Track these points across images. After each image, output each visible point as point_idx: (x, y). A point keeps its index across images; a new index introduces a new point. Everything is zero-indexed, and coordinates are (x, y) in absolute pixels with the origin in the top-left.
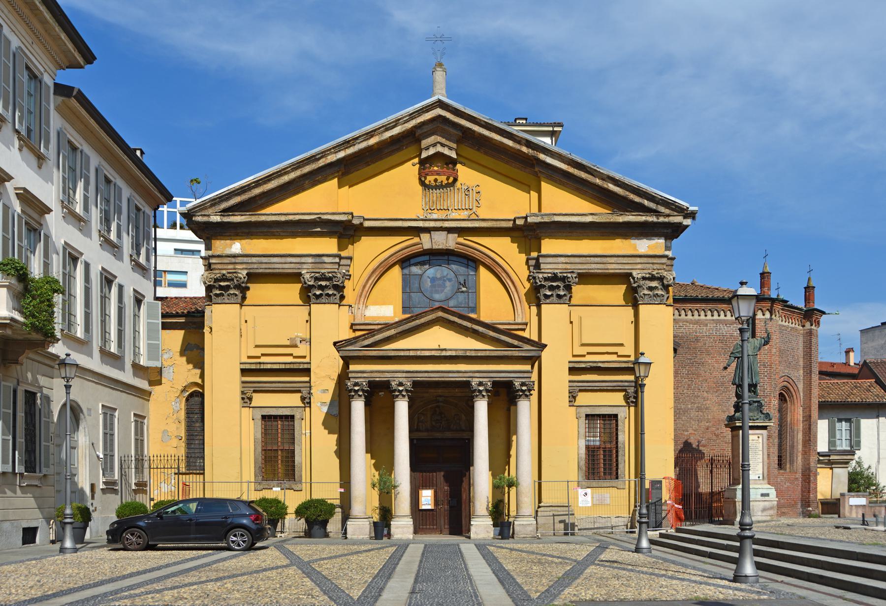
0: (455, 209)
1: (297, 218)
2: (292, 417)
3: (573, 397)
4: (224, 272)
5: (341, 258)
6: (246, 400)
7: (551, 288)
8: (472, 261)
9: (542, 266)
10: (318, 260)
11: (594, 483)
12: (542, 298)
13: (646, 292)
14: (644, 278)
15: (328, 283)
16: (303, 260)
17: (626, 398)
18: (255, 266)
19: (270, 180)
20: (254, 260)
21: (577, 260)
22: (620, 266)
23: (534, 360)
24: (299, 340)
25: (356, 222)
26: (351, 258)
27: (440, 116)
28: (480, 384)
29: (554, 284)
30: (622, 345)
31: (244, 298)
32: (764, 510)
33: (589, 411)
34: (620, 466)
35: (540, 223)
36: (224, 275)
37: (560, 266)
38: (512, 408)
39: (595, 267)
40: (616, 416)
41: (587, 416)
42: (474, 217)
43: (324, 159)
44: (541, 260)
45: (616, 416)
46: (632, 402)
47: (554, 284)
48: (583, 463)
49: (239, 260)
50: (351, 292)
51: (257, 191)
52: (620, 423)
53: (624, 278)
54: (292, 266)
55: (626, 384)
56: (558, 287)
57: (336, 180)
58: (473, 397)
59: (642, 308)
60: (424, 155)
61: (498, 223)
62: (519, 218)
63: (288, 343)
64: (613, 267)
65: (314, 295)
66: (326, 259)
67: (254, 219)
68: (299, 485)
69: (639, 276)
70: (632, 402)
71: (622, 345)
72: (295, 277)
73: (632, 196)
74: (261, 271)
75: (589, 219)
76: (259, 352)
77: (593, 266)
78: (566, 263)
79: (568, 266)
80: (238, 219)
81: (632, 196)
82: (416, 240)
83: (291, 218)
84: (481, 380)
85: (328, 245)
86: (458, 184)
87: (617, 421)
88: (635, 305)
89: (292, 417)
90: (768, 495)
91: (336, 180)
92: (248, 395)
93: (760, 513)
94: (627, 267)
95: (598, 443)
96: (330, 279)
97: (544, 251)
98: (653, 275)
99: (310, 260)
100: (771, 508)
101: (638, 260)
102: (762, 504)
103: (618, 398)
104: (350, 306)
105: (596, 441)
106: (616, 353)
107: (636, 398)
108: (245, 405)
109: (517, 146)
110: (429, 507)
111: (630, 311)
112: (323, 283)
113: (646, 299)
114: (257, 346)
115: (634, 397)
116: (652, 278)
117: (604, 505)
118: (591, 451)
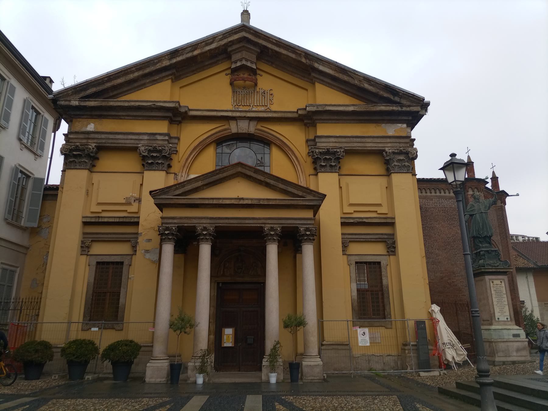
0: (255, 106)
1: (137, 104)
2: (122, 263)
3: (345, 246)
4: (78, 144)
5: (171, 138)
8: (266, 142)
9: (318, 144)
10: (152, 138)
13: (396, 164)
14: (394, 153)
15: (158, 155)
16: (141, 137)
18: (104, 141)
19: (119, 77)
20: (103, 136)
21: (344, 140)
22: (375, 145)
23: (316, 208)
24: (133, 199)
25: (183, 110)
28: (272, 229)
29: (327, 157)
31: (94, 166)
32: (518, 350)
33: (358, 259)
36: (77, 146)
37: (331, 145)
38: (298, 255)
39: (356, 145)
40: (379, 263)
41: (356, 263)
42: (268, 110)
43: (160, 64)
44: (317, 140)
45: (379, 263)
47: (327, 157)
48: (356, 304)
49: (92, 136)
50: (177, 164)
51: (109, 85)
52: (383, 270)
53: (379, 153)
54: (132, 141)
55: (386, 237)
56: (330, 159)
57: (170, 81)
58: (265, 242)
60: (233, 66)
61: (286, 114)
62: (300, 109)
63: (124, 201)
64: (370, 145)
65: (147, 163)
66: (159, 137)
69: (390, 151)
71: (380, 205)
72: (135, 149)
74: (108, 145)
75: (351, 109)
76: (99, 209)
77: (356, 145)
78: (336, 142)
83: (133, 104)
84: (272, 226)
85: (161, 127)
87: (380, 268)
89: (122, 263)
90: (517, 336)
92: (87, 244)
93: (515, 354)
94: (380, 145)
95: (367, 287)
96: (160, 151)
98: (401, 150)
99: (146, 137)
100: (524, 349)
101: (388, 140)
102: (516, 344)
104: (175, 174)
105: (365, 285)
106: (377, 211)
110: (230, 345)
112: (155, 155)
113: (396, 169)
114: (99, 204)
115: (392, 248)
116: (401, 153)
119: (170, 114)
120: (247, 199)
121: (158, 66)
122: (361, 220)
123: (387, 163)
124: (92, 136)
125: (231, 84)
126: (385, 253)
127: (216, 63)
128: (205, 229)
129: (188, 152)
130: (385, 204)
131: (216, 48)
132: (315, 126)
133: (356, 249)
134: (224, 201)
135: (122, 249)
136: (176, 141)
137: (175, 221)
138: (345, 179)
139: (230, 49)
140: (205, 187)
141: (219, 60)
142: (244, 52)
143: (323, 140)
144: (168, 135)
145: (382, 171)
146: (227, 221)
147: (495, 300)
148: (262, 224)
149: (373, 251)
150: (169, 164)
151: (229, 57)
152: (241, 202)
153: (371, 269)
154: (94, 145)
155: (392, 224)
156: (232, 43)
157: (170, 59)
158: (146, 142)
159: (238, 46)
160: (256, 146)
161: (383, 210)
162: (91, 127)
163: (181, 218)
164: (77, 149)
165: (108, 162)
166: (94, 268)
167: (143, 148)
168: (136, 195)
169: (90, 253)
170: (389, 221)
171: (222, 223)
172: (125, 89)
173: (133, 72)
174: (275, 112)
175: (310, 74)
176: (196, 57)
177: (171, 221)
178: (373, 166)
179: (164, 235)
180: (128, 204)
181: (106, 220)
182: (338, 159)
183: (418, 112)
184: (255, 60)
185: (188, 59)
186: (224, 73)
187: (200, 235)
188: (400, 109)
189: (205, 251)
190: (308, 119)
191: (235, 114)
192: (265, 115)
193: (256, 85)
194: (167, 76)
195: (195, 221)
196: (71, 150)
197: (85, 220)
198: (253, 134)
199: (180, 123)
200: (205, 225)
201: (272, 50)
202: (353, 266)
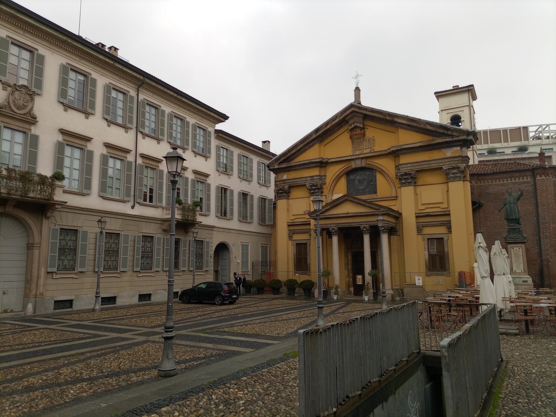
1: (303, 162)
5: (322, 176)
13: (451, 176)
14: (449, 169)
16: (307, 179)
20: (291, 181)
21: (416, 164)
25: (325, 161)
33: (429, 237)
37: (409, 168)
39: (425, 167)
41: (428, 239)
48: (427, 263)
49: (286, 181)
50: (326, 191)
51: (289, 154)
52: (445, 242)
64: (434, 166)
66: (315, 178)
71: (442, 203)
75: (418, 145)
79: (412, 168)
80: (283, 166)
85: (315, 172)
95: (435, 253)
96: (316, 186)
99: (309, 179)
101: (446, 160)
105: (434, 251)
113: (452, 179)
116: (454, 168)
118: (432, 257)
119: (319, 164)
121: (310, 139)
123: (447, 174)
124: (286, 181)
127: (341, 127)
128: (333, 229)
130: (446, 202)
133: (428, 231)
136: (324, 177)
138: (419, 189)
142: (356, 119)
143: (404, 166)
145: (445, 181)
154: (287, 186)
155: (449, 215)
157: (316, 134)
160: (367, 173)
162: (285, 177)
164: (280, 190)
165: (295, 193)
171: (341, 226)
173: (299, 145)
174: (375, 152)
176: (329, 128)
182: (414, 178)
185: (324, 132)
188: (451, 139)
189: (335, 239)
190: (395, 154)
192: (369, 155)
196: (278, 191)
199: (325, 166)
202: (426, 241)
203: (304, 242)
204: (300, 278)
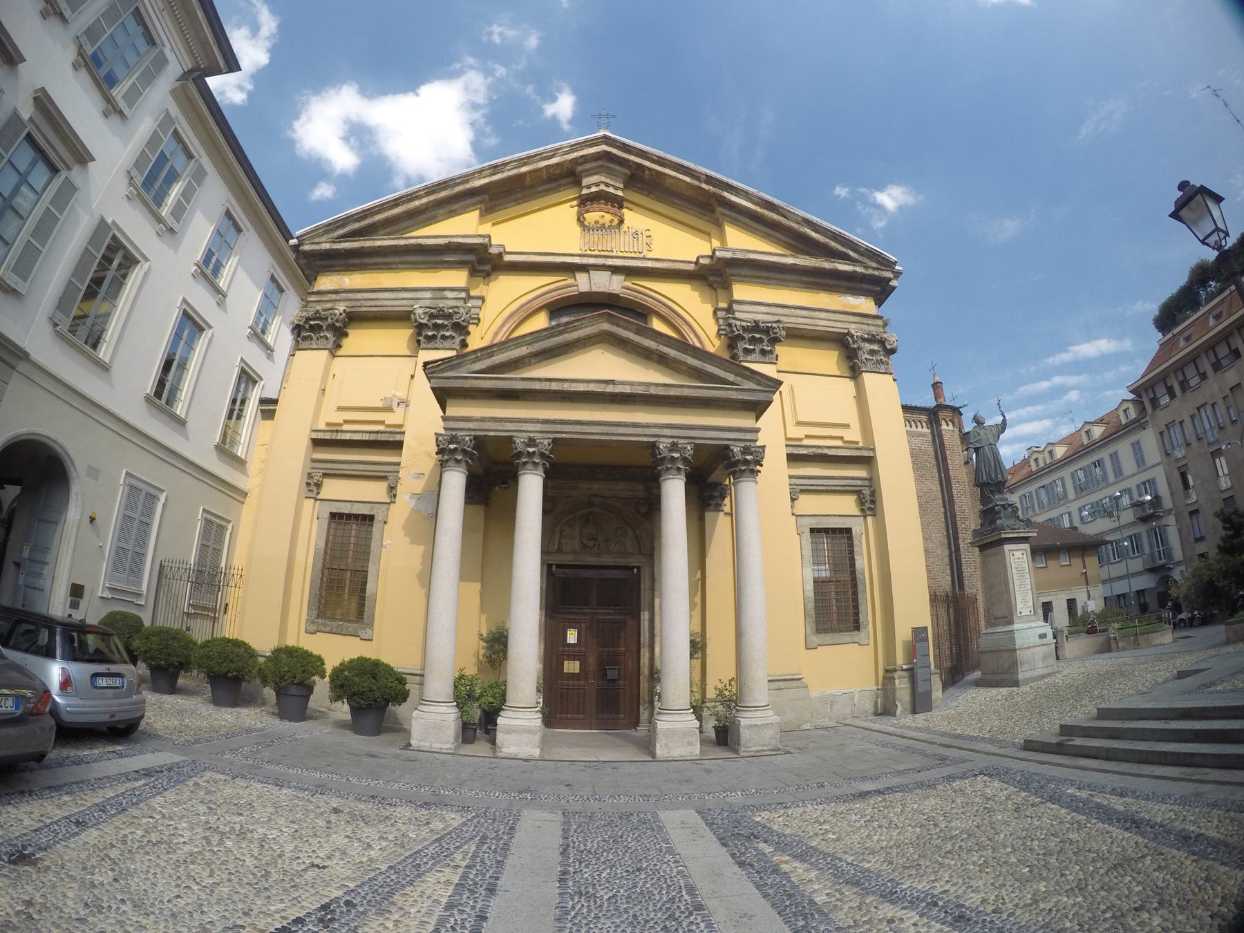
2: (371, 518)
5: (470, 297)
6: (313, 488)
7: (753, 340)
10: (438, 294)
11: (828, 638)
12: (741, 353)
14: (864, 340)
16: (419, 295)
17: (861, 503)
18: (358, 304)
19: (397, 205)
20: (359, 296)
22: (832, 324)
25: (493, 251)
26: (483, 299)
27: (606, 152)
29: (757, 336)
30: (847, 426)
31: (339, 346)
33: (815, 523)
34: (862, 608)
35: (732, 259)
36: (317, 312)
39: (802, 322)
40: (849, 531)
41: (812, 530)
44: (735, 307)
45: (849, 531)
46: (870, 509)
47: (757, 336)
48: (811, 605)
54: (405, 302)
55: (859, 483)
57: (477, 212)
59: (868, 378)
60: (585, 191)
63: (380, 405)
64: (824, 324)
66: (450, 294)
67: (368, 244)
68: (369, 631)
70: (870, 509)
71: (847, 426)
73: (833, 244)
76: (339, 418)
81: (833, 244)
82: (570, 281)
85: (456, 278)
86: (624, 227)
87: (850, 539)
88: (854, 373)
89: (371, 518)
91: (477, 212)
96: (449, 316)
97: (736, 297)
99: (428, 295)
103: (848, 505)
107: (873, 502)
108: (310, 495)
109: (696, 183)
111: (849, 385)
112: (439, 322)
113: (870, 366)
114: (340, 409)
115: (869, 501)
117: (844, 673)
120: (622, 383)
122: (819, 451)
125: (580, 221)
126: (858, 513)
128: (532, 442)
129: (499, 322)
131: (557, 165)
132: (727, 287)
133: (809, 504)
134: (574, 385)
135: (374, 491)
136: (479, 303)
137: (471, 425)
139: (580, 168)
140: (533, 360)
141: (560, 186)
144: (466, 290)
146: (578, 428)
147: (1016, 583)
148: (652, 436)
149: (842, 508)
150: (463, 340)
151: (578, 183)
152: (610, 389)
153: (834, 540)
154: (342, 309)
156: (585, 159)
158: (428, 303)
159: (594, 164)
161: (854, 435)
163: (482, 420)
166: (325, 525)
167: (420, 311)
168: (401, 394)
169: (319, 497)
170: (865, 453)
172: (404, 224)
175: (713, 211)
177: (461, 425)
178: (828, 359)
179: (446, 453)
180: (388, 409)
181: (348, 436)
183: (890, 280)
184: (621, 186)
185: (510, 178)
186: (568, 205)
187: (519, 455)
189: (531, 487)
191: (585, 261)
193: (621, 221)
194: (473, 205)
195: (511, 426)
197: (314, 436)
198: (617, 296)
200: (532, 435)
201: (650, 169)
203: (364, 510)
204: (334, 650)
